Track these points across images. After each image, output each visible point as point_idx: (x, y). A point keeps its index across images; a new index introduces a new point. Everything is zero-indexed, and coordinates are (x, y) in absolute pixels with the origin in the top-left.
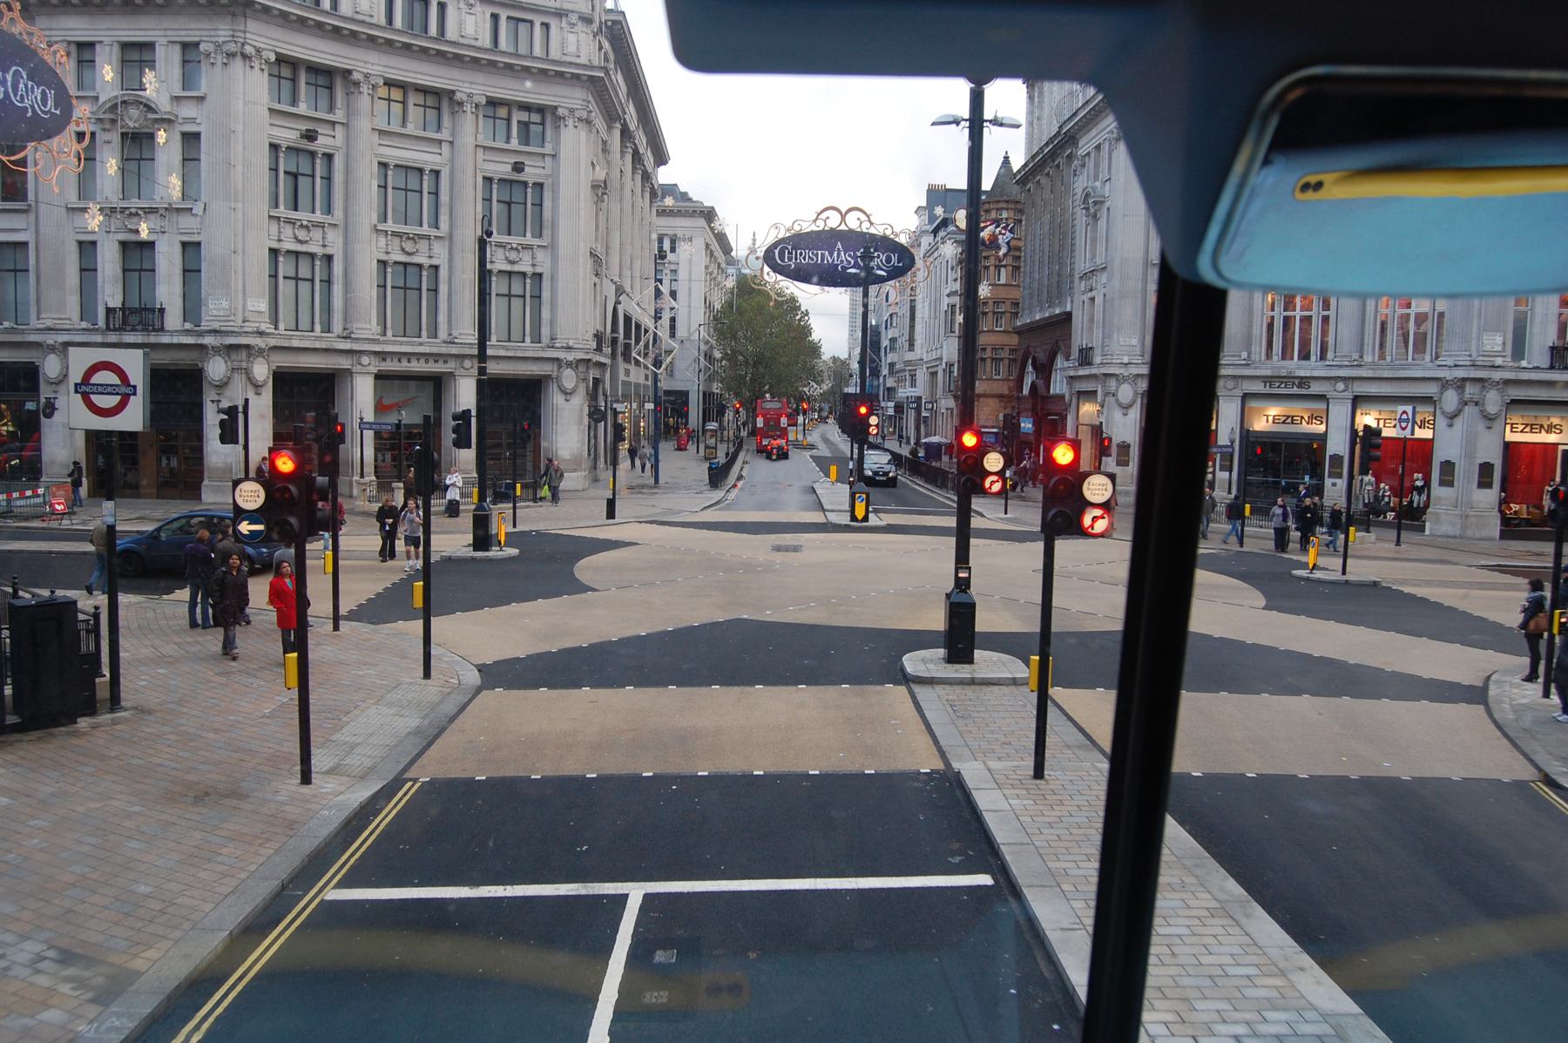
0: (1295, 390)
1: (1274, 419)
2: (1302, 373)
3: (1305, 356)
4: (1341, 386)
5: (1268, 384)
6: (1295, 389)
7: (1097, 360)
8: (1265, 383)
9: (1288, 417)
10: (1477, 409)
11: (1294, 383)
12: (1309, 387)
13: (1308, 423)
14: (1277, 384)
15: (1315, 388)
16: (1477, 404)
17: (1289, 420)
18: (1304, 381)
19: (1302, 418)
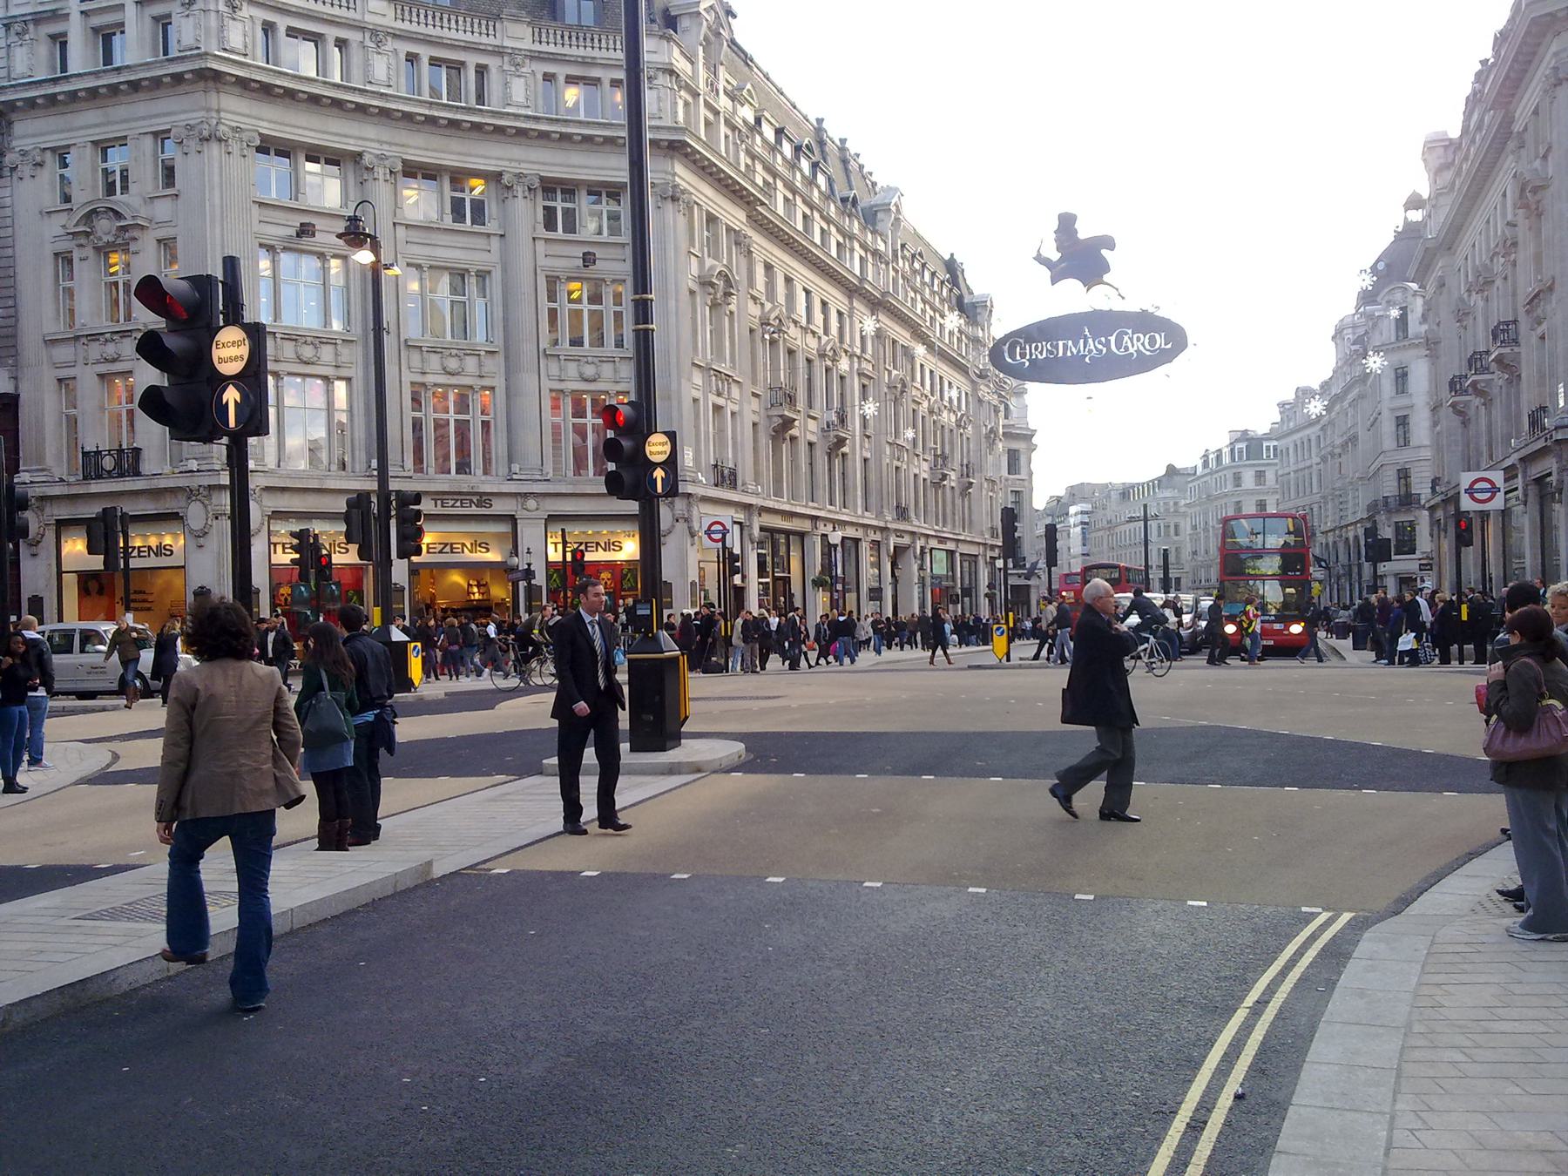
0: (474, 510)
1: (428, 548)
2: (487, 488)
3: (463, 467)
4: (531, 504)
5: (439, 502)
6: (474, 507)
7: (147, 467)
8: (436, 500)
9: (446, 545)
10: (686, 525)
11: (471, 501)
12: (491, 505)
13: (471, 552)
14: (451, 503)
15: (499, 507)
16: (686, 520)
17: (448, 549)
18: (484, 498)
19: (463, 545)
